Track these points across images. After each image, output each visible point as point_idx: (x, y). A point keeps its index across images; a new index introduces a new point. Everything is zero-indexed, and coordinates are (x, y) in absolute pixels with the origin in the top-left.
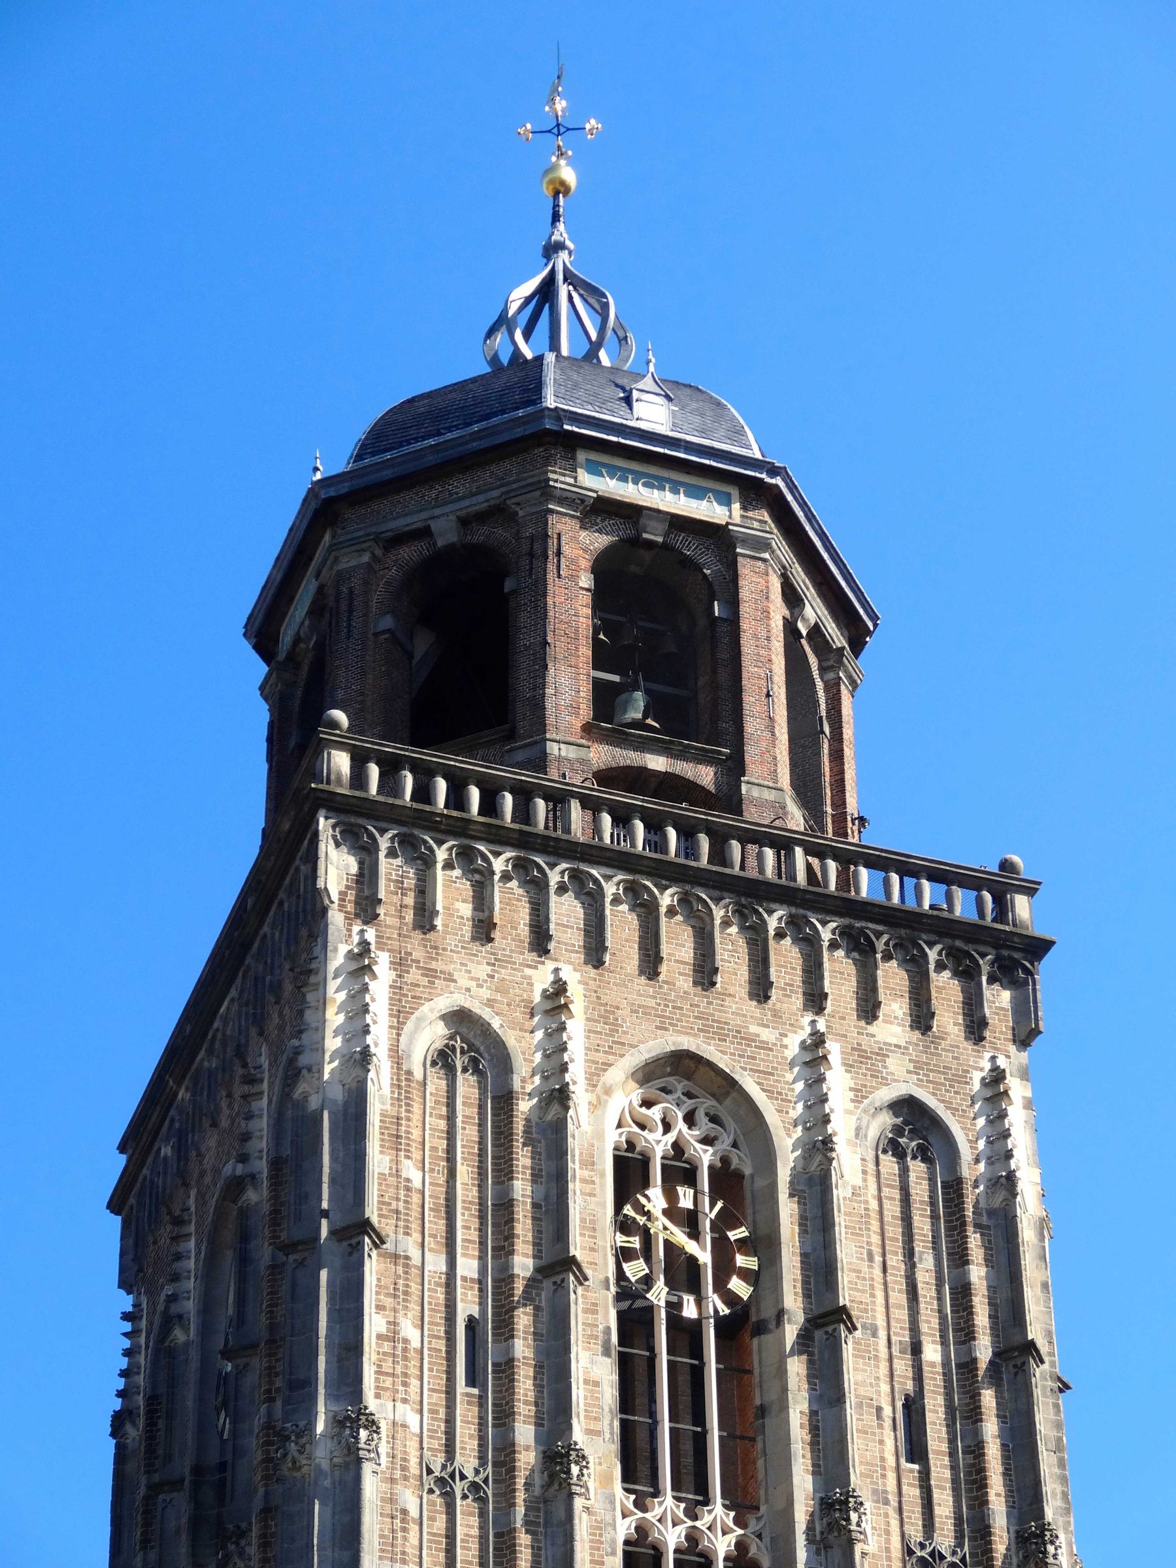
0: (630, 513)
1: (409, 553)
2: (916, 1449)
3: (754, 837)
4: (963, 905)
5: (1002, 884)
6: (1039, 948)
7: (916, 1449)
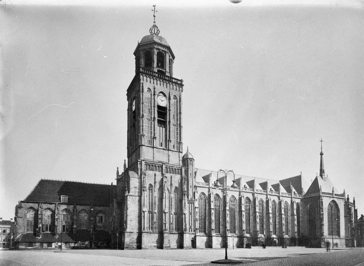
0: (160, 49)
1: (145, 51)
2: (174, 118)
3: (167, 76)
4: (179, 82)
5: (181, 81)
6: (183, 85)
7: (174, 118)
